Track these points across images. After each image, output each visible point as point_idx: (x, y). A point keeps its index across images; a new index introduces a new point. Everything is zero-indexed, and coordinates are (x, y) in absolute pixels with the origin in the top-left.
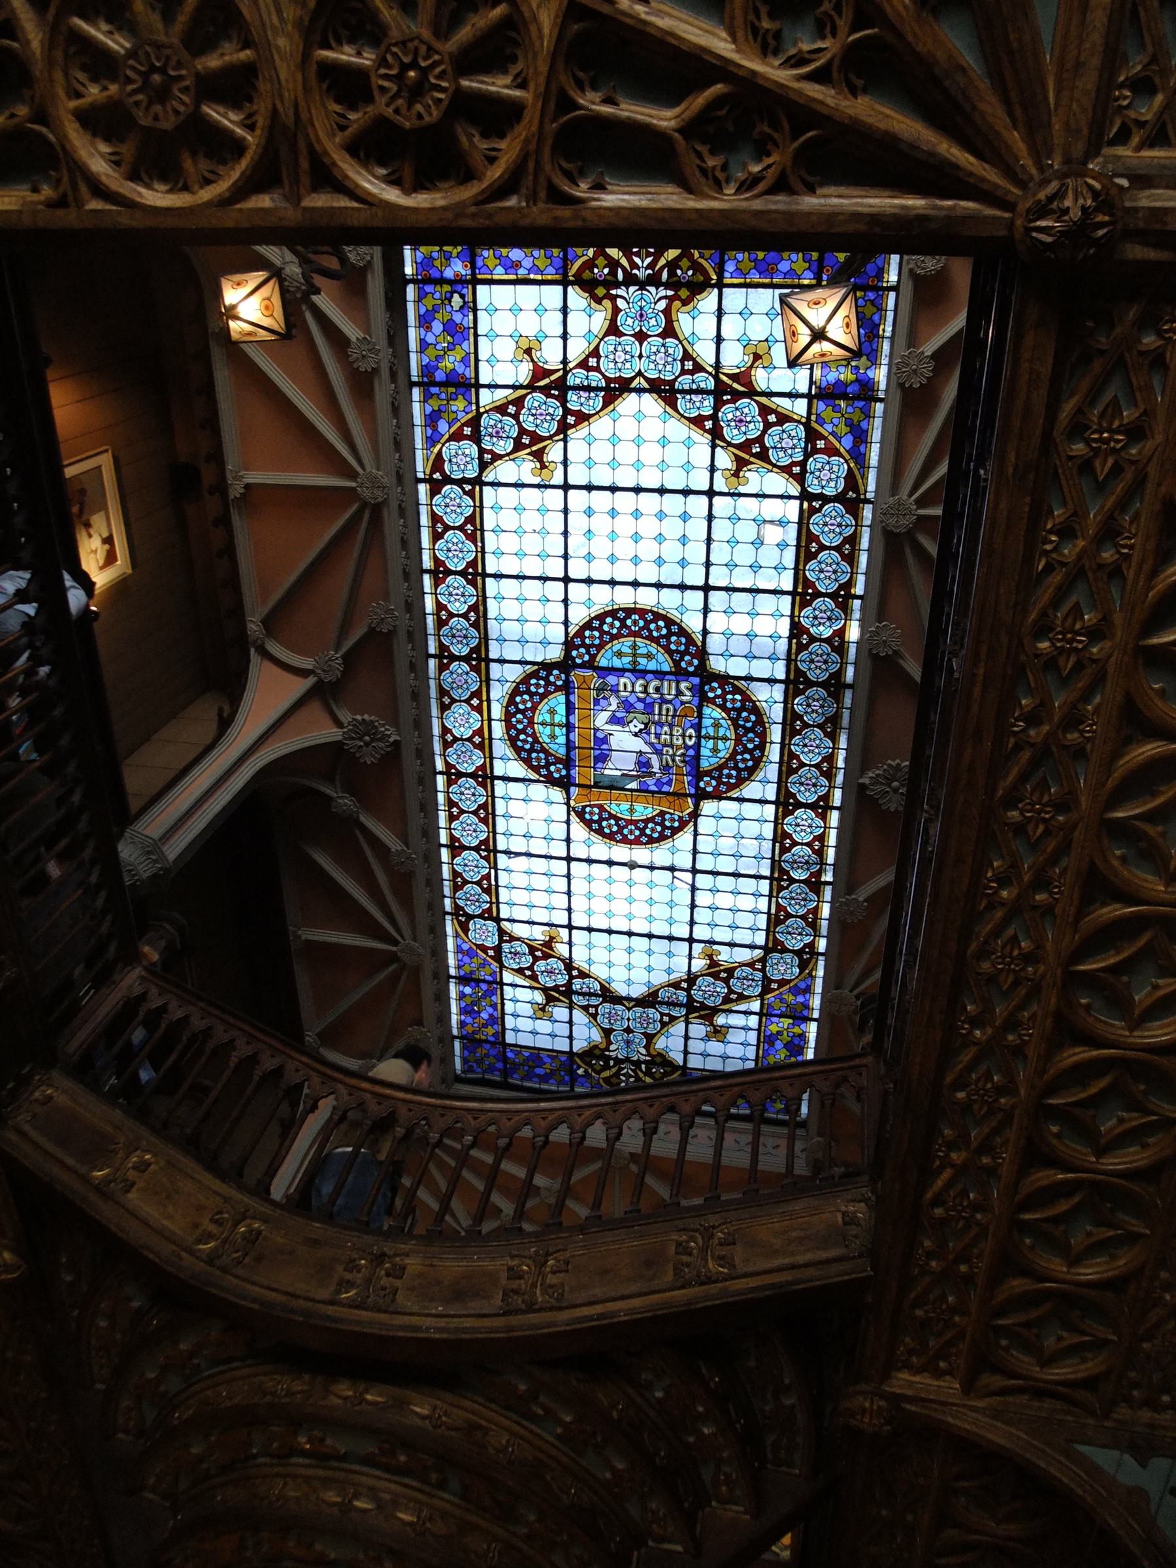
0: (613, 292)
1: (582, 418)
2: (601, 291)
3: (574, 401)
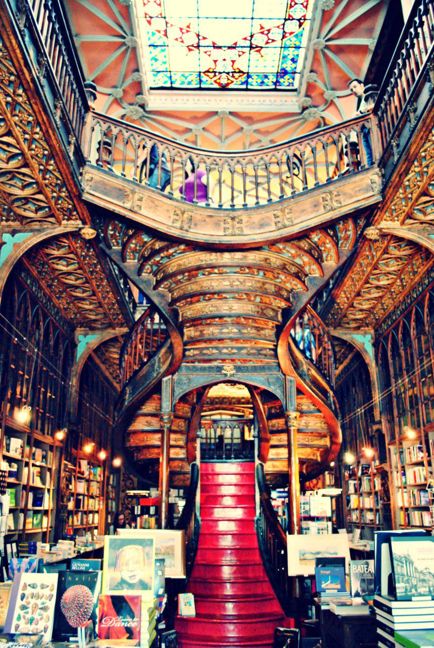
0: (233, 71)
1: (245, 39)
2: (237, 71)
3: (248, 43)
